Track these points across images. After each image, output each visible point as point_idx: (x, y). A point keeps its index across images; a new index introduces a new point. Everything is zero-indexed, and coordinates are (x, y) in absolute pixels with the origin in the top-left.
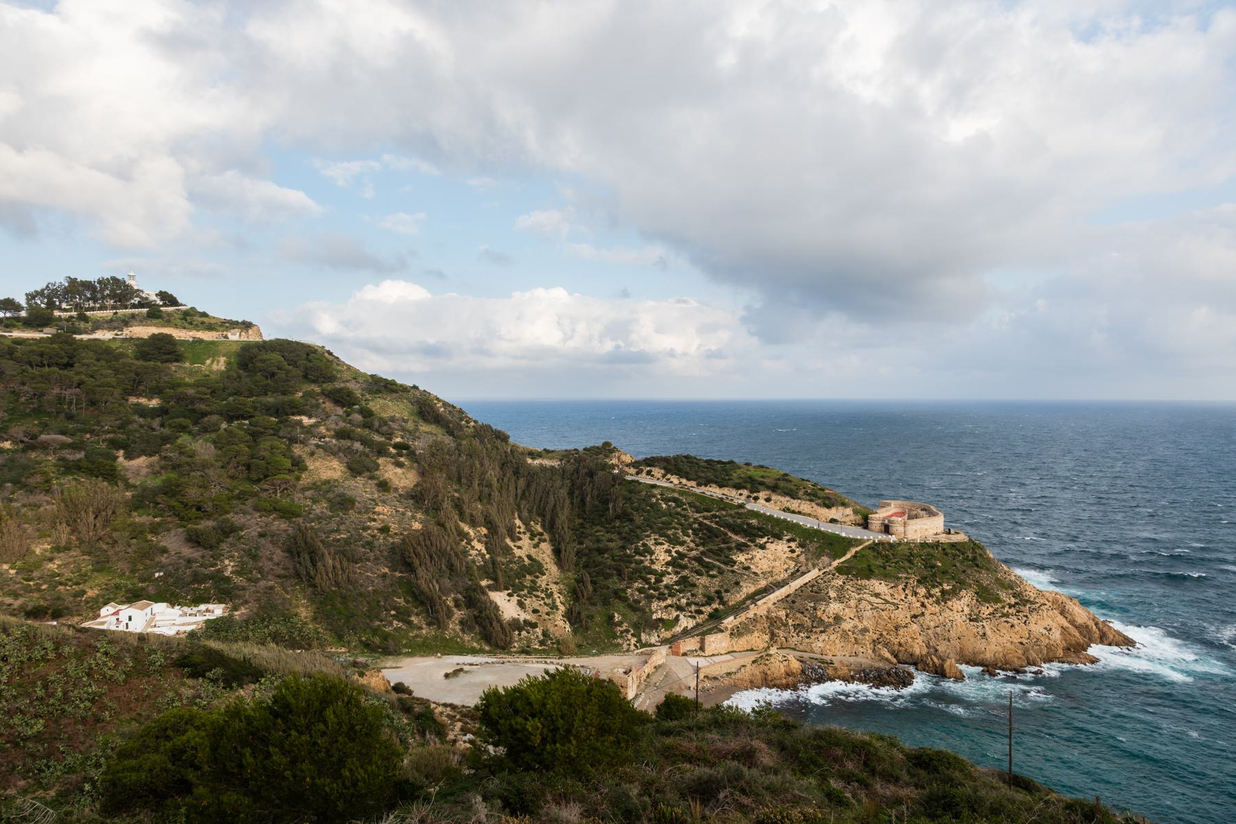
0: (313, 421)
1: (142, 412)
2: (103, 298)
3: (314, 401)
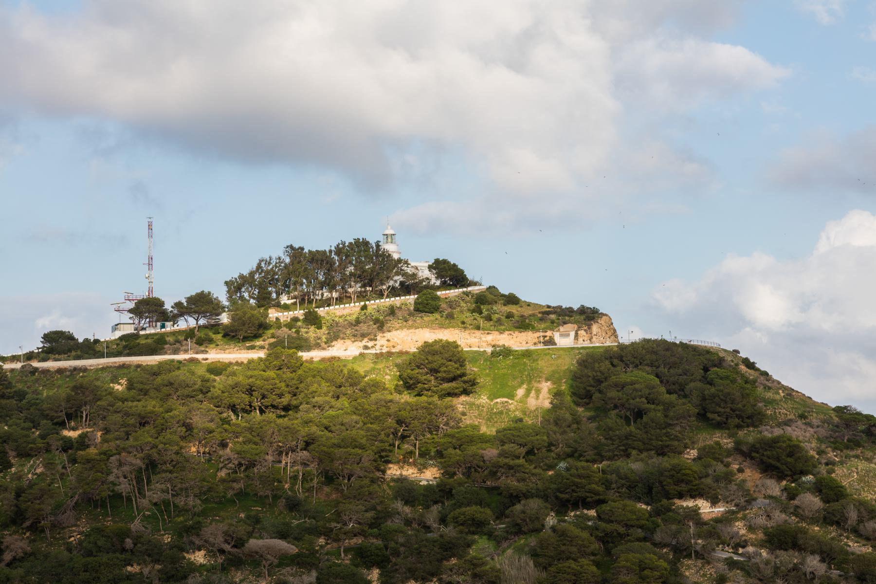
0: (720, 509)
1: (407, 492)
2: (345, 280)
3: (720, 468)
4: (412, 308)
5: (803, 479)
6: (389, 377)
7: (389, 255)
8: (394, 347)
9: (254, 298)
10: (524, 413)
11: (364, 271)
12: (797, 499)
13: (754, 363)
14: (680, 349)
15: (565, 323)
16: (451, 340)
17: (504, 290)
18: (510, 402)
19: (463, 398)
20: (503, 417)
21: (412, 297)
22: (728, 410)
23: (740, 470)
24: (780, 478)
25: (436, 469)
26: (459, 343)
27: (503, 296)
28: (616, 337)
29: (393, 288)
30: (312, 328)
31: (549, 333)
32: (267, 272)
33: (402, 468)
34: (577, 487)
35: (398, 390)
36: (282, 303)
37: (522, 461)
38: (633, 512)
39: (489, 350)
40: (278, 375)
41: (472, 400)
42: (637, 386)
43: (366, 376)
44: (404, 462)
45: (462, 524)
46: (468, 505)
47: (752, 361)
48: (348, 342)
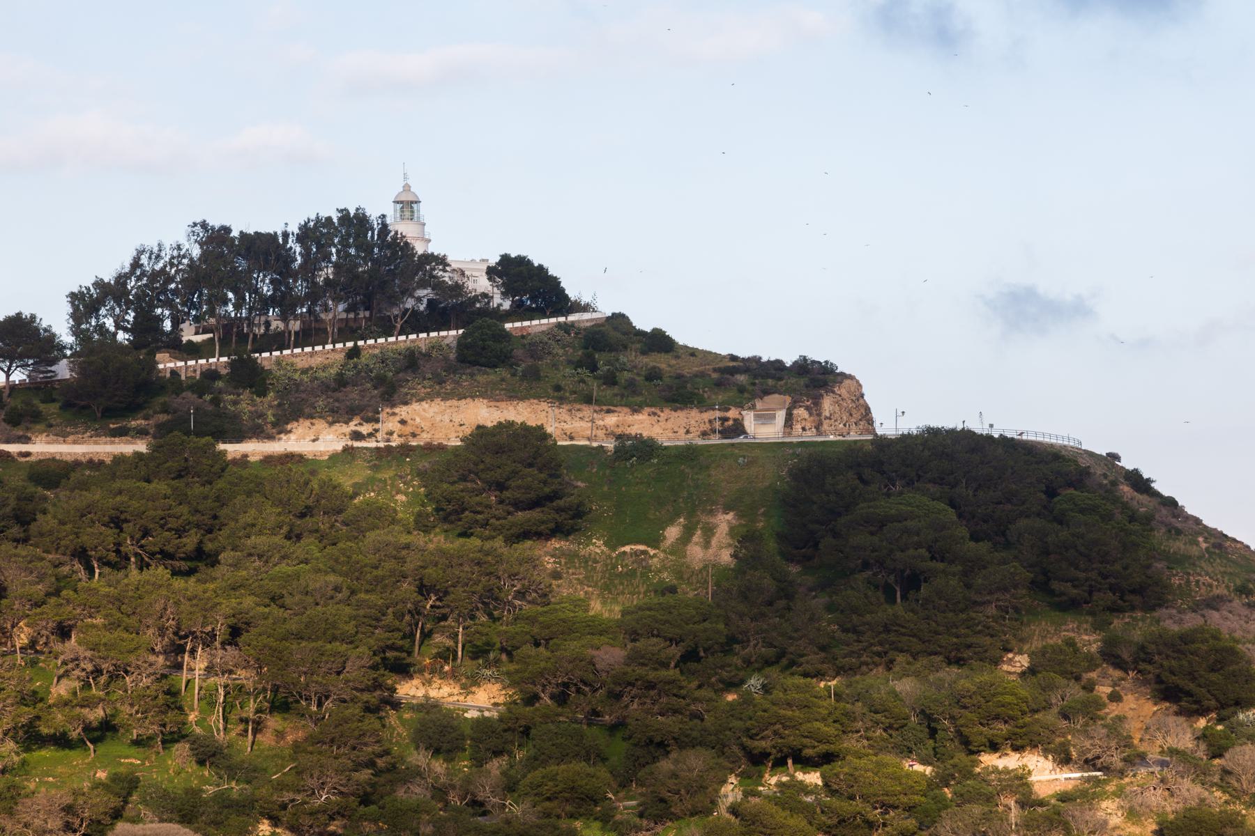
0: (1068, 778)
1: (441, 733)
2: (314, 295)
3: (1074, 692)
4: (452, 356)
5: (1241, 716)
6: (403, 498)
7: (407, 244)
8: (414, 435)
9: (125, 330)
10: (679, 575)
11: (357, 276)
12: (1227, 755)
13: (1149, 480)
14: (1000, 451)
15: (767, 392)
16: (532, 423)
17: (643, 323)
18: (652, 552)
19: (555, 544)
20: (636, 582)
21: (453, 333)
22: (1094, 575)
23: (1115, 698)
24: (1192, 713)
25: (498, 686)
26: (549, 430)
27: (642, 333)
28: (870, 422)
29: (415, 313)
30: (246, 395)
31: (733, 413)
32: (155, 275)
33: (430, 682)
34: (785, 727)
35: (423, 525)
36: (185, 339)
37: (672, 673)
38: (897, 778)
39: (610, 445)
40: (175, 489)
41: (573, 547)
42: (909, 523)
43: (356, 495)
44: (432, 672)
45: (549, 799)
46: (561, 759)
47: (1145, 476)
48: (320, 425)
